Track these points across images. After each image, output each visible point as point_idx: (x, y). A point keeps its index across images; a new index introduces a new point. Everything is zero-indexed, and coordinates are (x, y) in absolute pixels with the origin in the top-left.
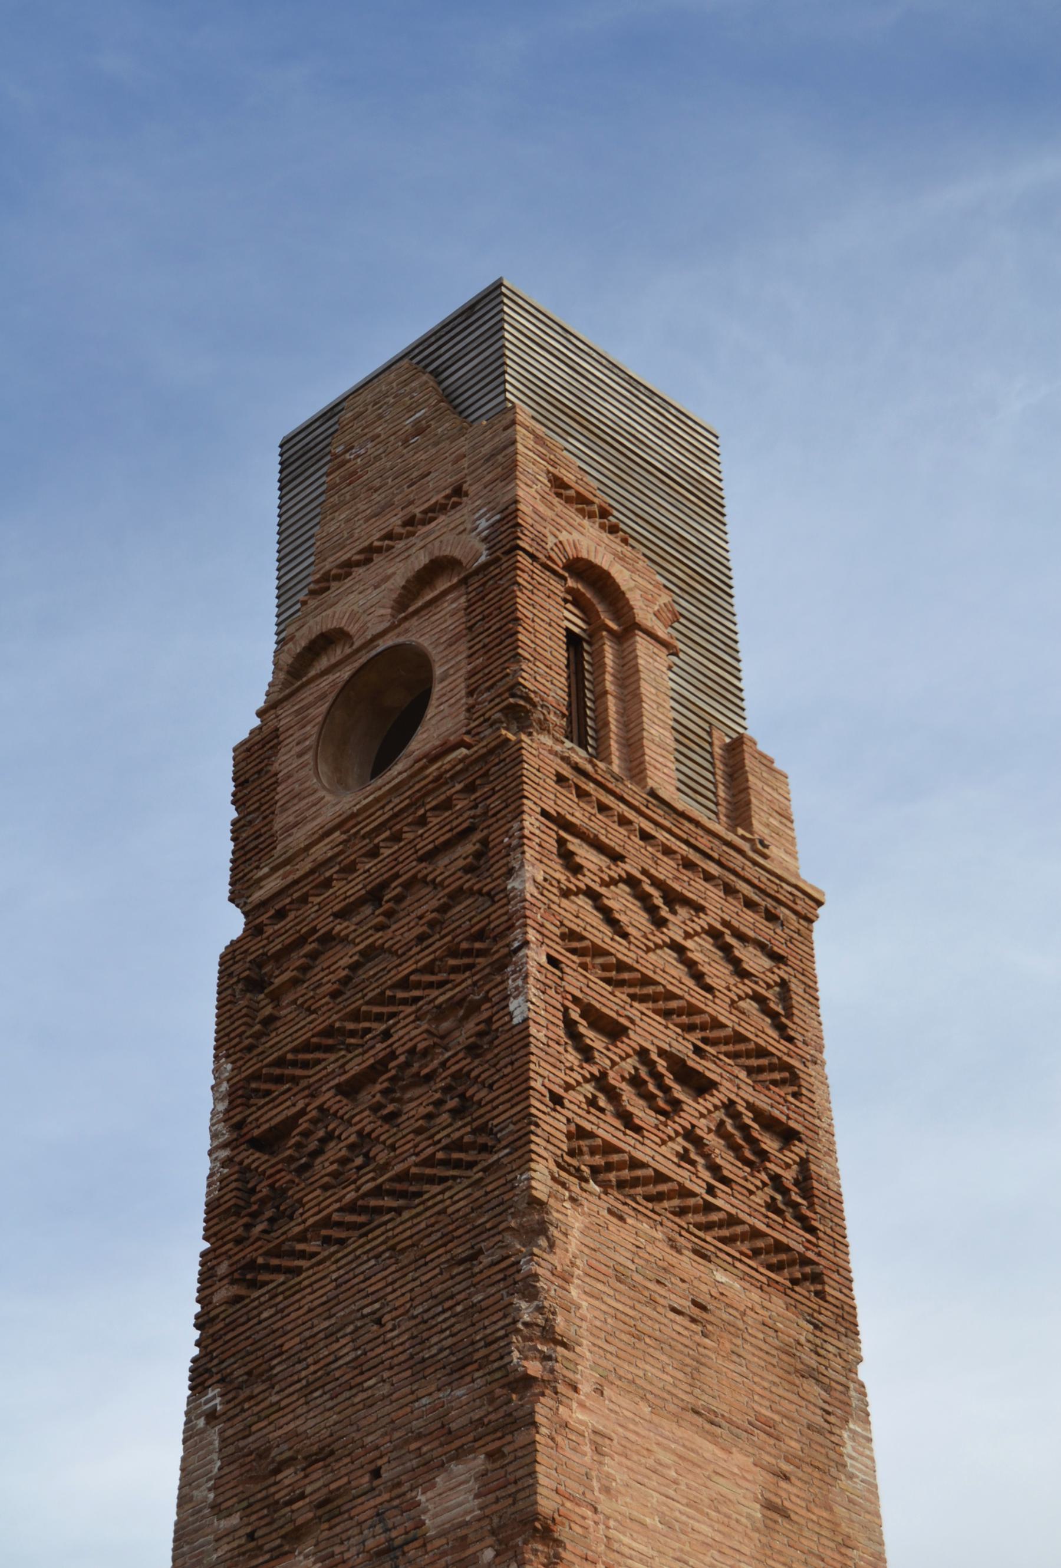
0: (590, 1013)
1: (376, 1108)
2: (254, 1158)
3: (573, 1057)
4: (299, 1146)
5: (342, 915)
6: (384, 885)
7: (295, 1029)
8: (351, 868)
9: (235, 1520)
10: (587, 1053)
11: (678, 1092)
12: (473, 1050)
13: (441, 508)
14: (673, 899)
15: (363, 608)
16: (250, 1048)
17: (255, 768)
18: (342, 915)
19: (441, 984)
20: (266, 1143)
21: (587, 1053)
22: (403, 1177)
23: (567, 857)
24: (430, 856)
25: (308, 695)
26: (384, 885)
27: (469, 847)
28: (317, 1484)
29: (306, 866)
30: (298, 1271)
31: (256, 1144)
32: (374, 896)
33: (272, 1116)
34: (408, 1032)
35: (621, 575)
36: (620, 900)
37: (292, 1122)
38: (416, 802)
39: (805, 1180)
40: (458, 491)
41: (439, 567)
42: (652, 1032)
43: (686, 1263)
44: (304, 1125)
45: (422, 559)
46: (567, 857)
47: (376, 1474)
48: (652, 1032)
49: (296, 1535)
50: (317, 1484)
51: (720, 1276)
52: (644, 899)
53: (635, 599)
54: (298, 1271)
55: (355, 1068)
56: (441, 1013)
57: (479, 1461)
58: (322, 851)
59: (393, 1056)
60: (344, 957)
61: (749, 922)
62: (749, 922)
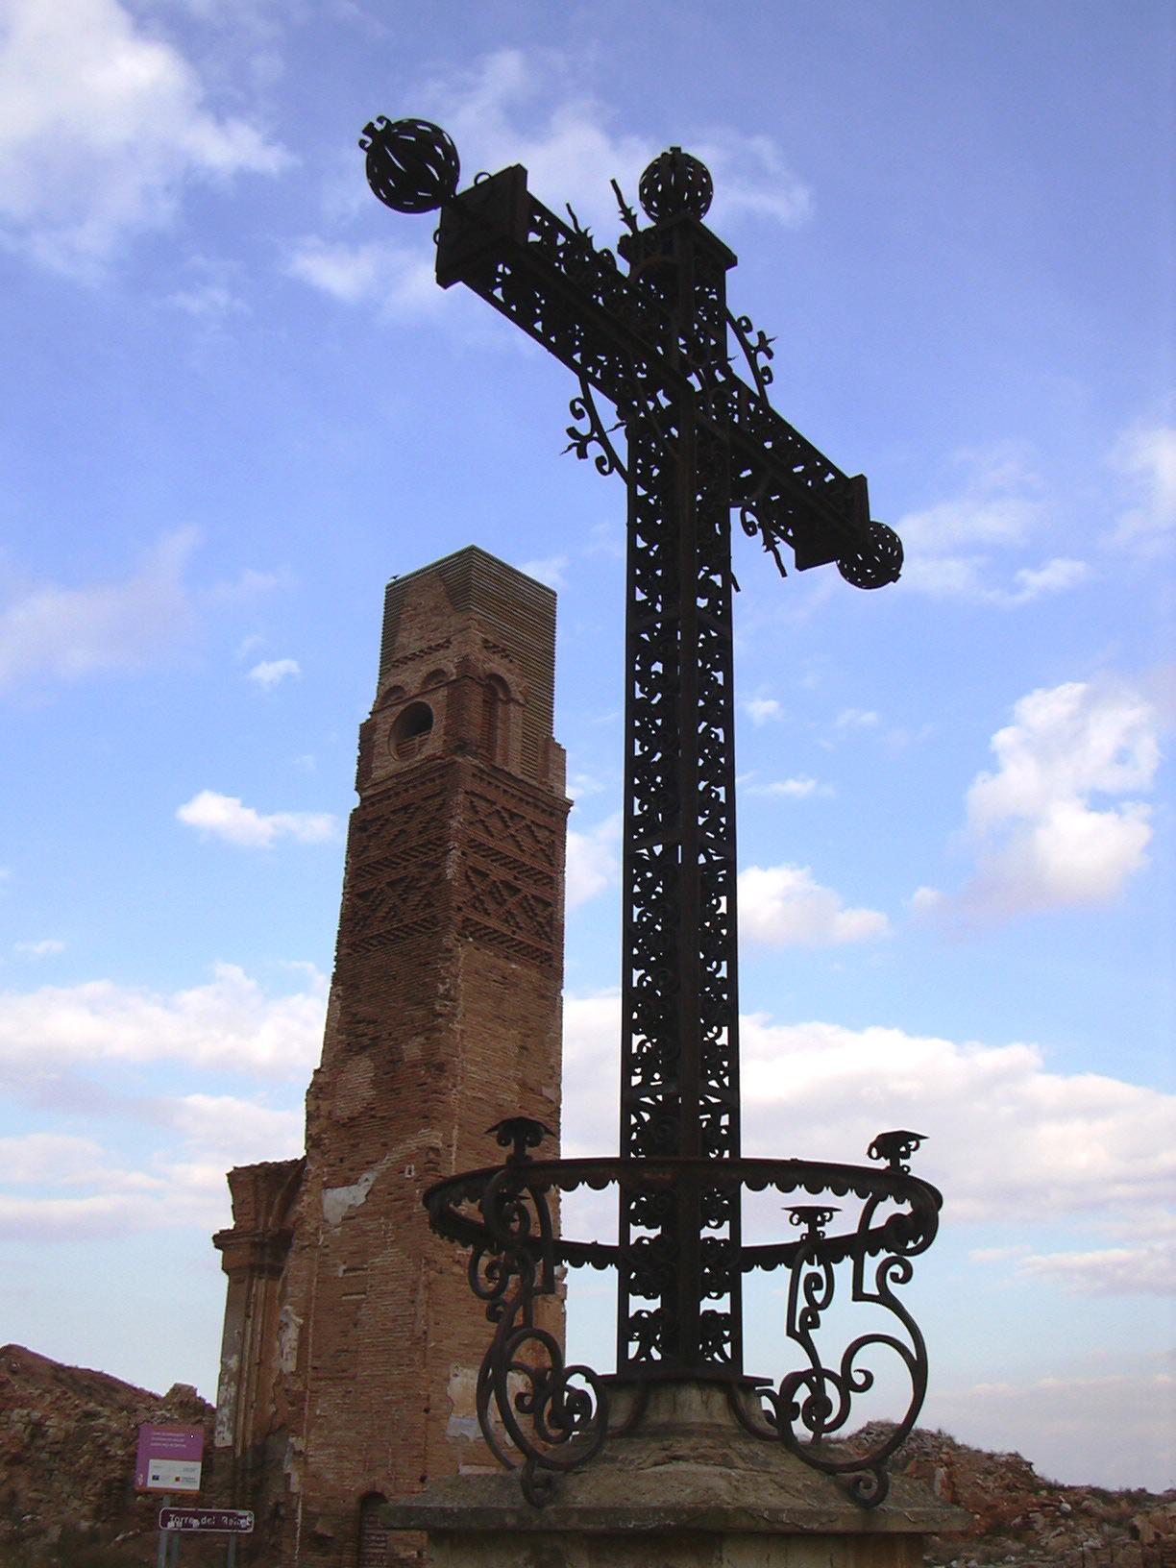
0: (475, 871)
2: (356, 901)
3: (467, 890)
5: (393, 812)
7: (374, 853)
8: (397, 794)
10: (473, 887)
11: (504, 893)
12: (433, 884)
13: (440, 646)
14: (512, 815)
15: (410, 679)
17: (367, 731)
18: (393, 812)
20: (361, 896)
21: (473, 887)
23: (474, 809)
25: (387, 712)
27: (438, 801)
29: (382, 788)
31: (359, 896)
32: (405, 808)
33: (365, 887)
35: (507, 677)
36: (495, 824)
38: (423, 775)
39: (550, 923)
40: (448, 641)
41: (438, 673)
42: (499, 873)
43: (501, 962)
45: (432, 668)
46: (474, 809)
48: (499, 873)
49: (364, 1048)
50: (371, 1030)
52: (502, 818)
53: (513, 688)
55: (394, 877)
57: (421, 1039)
58: (389, 784)
60: (395, 830)
61: (541, 819)
62: (541, 819)
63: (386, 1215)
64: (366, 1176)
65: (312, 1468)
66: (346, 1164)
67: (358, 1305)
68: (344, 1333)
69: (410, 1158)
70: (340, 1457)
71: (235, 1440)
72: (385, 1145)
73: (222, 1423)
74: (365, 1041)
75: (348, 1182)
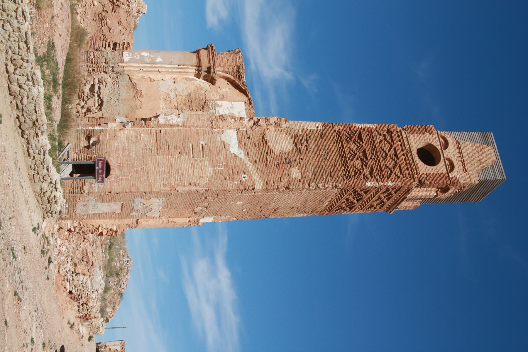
1: (360, 157)
4: (357, 142)
6: (397, 157)
9: (301, 133)
16: (377, 131)
19: (377, 169)
22: (347, 162)
24: (400, 166)
26: (397, 157)
28: (303, 148)
30: (337, 143)
32: (396, 155)
34: (370, 163)
37: (362, 140)
44: (361, 143)
47: (302, 159)
50: (303, 148)
51: (327, 203)
54: (337, 143)
56: (372, 168)
59: (367, 160)
63: (227, 166)
64: (242, 152)
65: (118, 133)
66: (247, 141)
67: (188, 154)
68: (176, 147)
69: (250, 177)
70: (124, 149)
71: (126, 63)
72: (255, 162)
73: (133, 55)
74: (299, 146)
75: (240, 142)
